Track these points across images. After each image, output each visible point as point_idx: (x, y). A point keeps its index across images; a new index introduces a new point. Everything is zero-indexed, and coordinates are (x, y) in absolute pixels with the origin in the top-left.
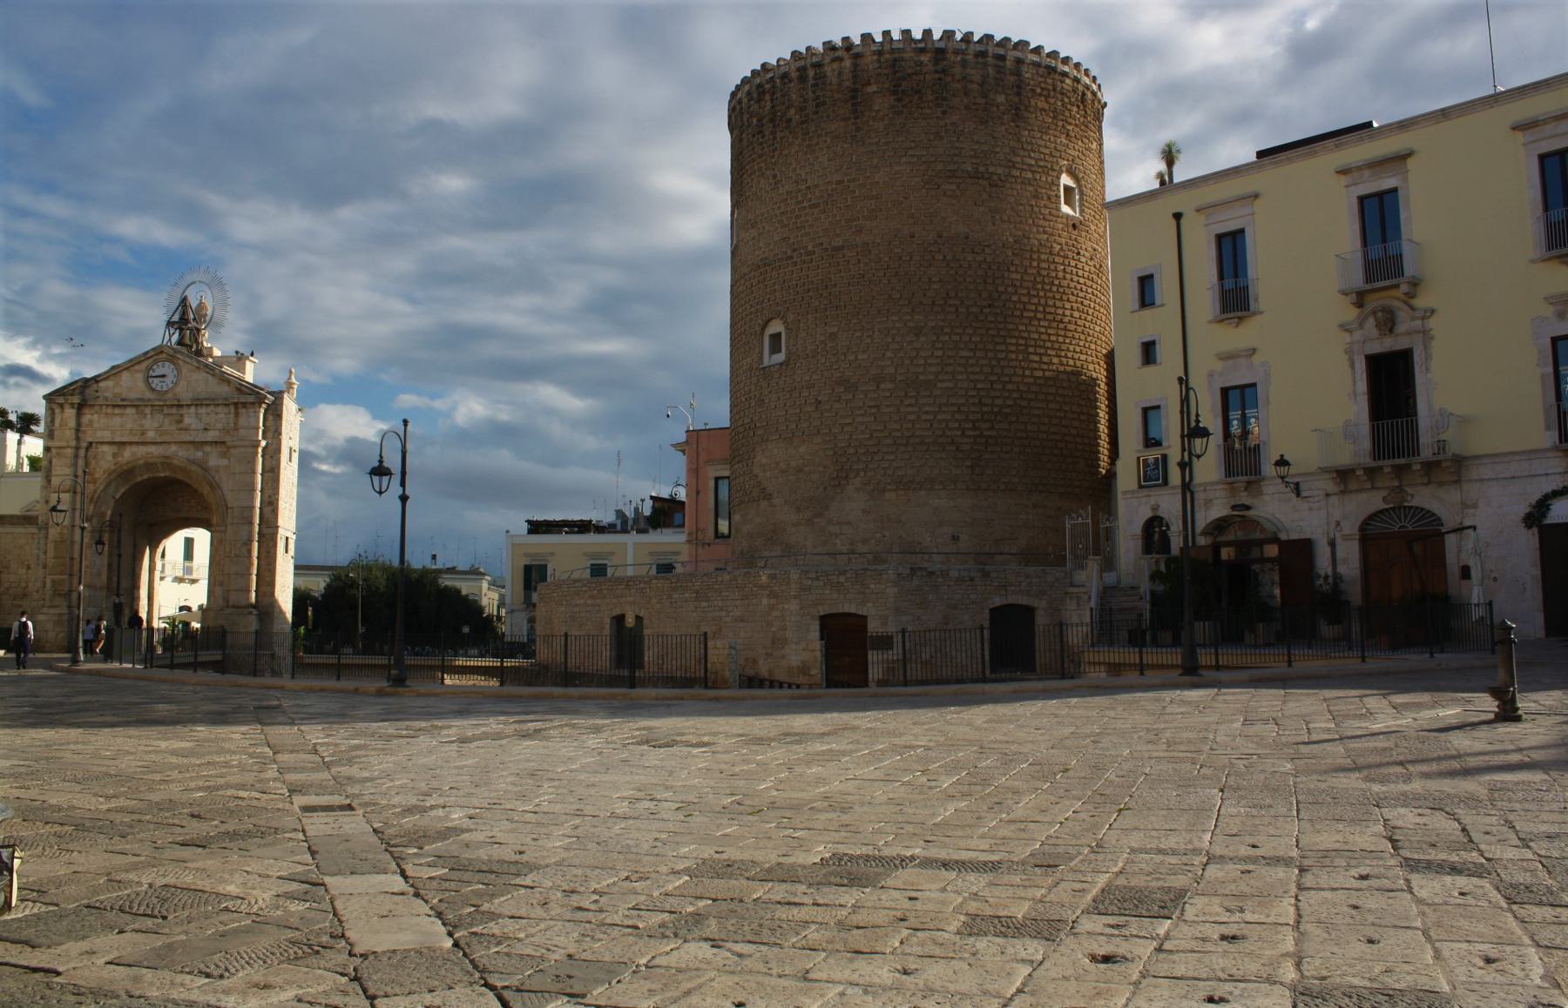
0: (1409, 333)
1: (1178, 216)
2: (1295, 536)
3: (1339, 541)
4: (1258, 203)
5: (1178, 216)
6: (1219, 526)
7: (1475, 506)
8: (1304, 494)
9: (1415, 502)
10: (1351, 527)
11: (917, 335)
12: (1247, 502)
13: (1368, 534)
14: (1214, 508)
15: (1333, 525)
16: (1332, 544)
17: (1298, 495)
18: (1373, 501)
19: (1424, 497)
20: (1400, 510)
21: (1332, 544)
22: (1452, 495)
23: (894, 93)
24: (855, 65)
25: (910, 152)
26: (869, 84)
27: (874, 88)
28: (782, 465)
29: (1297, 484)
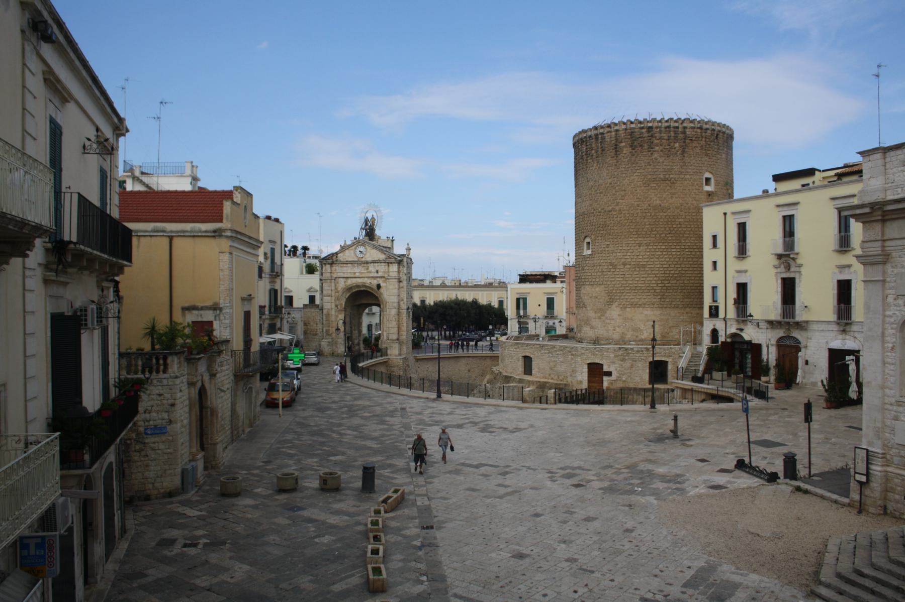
0: (795, 272)
1: (725, 214)
2: (757, 342)
3: (770, 346)
4: (750, 213)
5: (725, 214)
6: (734, 335)
7: (811, 339)
8: (760, 327)
9: (793, 335)
10: (774, 341)
11: (640, 246)
12: (742, 327)
13: (781, 344)
14: (732, 330)
15: (768, 340)
16: (768, 346)
17: (758, 327)
18: (780, 333)
19: (796, 334)
20: (788, 337)
21: (768, 346)
22: (804, 334)
23: (631, 146)
24: (616, 134)
25: (638, 171)
26: (621, 142)
27: (624, 144)
28: (590, 295)
29: (758, 323)
